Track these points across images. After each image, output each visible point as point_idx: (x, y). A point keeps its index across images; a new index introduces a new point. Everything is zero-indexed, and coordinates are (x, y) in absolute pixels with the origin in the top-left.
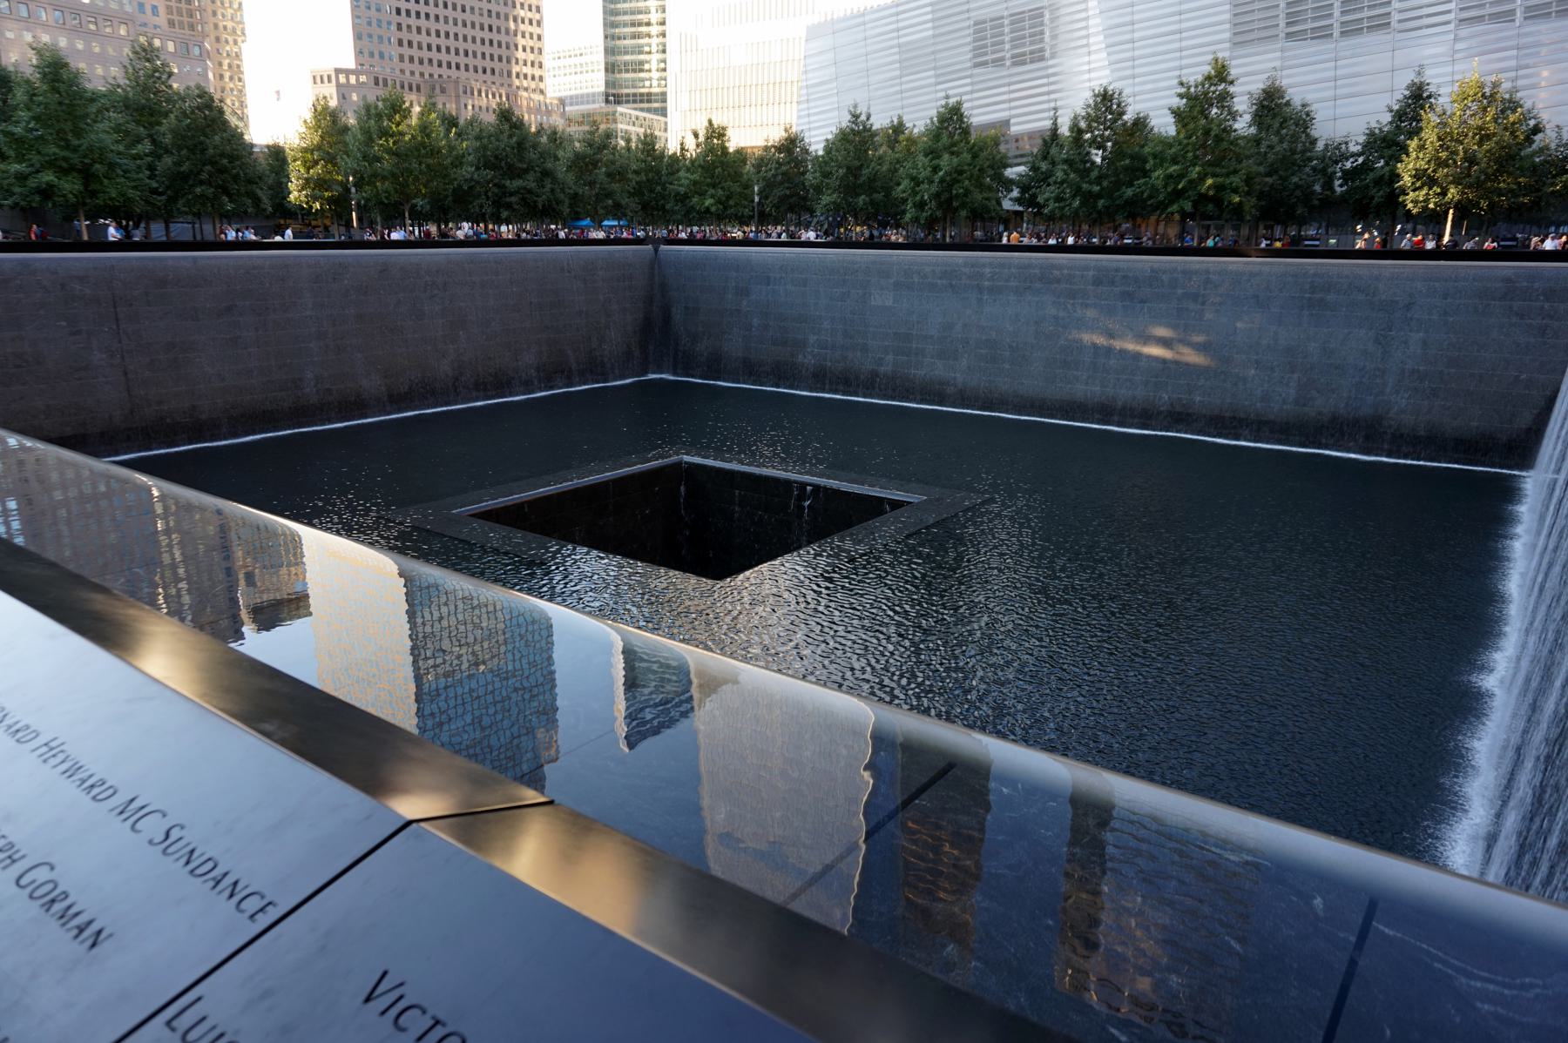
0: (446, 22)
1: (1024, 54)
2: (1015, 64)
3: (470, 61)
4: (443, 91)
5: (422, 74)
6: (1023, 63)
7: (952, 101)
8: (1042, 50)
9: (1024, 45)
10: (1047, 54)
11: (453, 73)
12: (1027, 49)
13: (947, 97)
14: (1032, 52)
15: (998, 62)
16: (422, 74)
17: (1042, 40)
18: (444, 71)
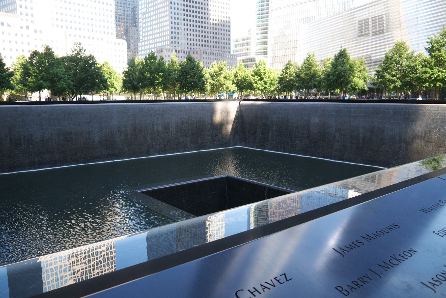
0: (199, 32)
1: (376, 31)
2: (373, 35)
3: (206, 44)
4: (197, 53)
5: (191, 48)
6: (376, 35)
7: (343, 48)
8: (383, 30)
9: (377, 28)
10: (385, 31)
11: (201, 47)
12: (377, 30)
13: (342, 47)
14: (379, 31)
15: (367, 35)
16: (191, 48)
17: (383, 26)
18: (198, 47)
